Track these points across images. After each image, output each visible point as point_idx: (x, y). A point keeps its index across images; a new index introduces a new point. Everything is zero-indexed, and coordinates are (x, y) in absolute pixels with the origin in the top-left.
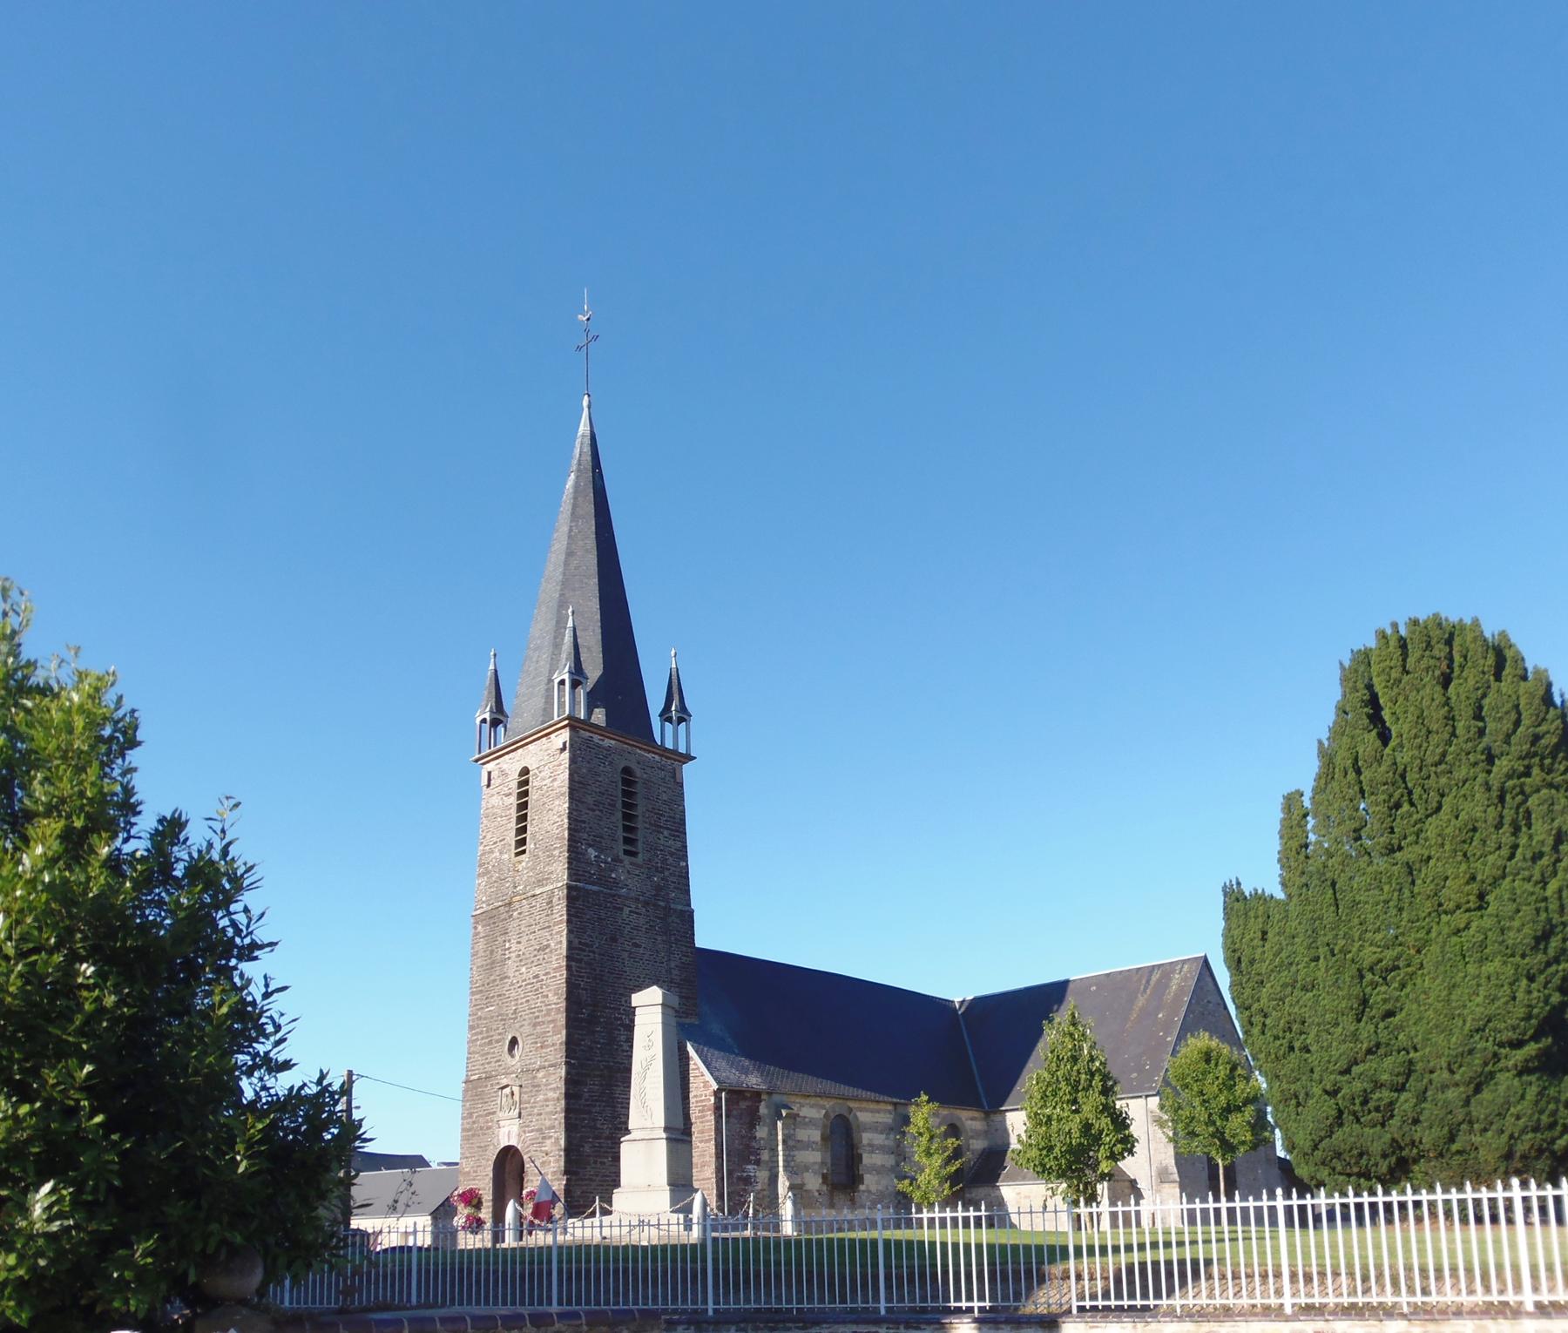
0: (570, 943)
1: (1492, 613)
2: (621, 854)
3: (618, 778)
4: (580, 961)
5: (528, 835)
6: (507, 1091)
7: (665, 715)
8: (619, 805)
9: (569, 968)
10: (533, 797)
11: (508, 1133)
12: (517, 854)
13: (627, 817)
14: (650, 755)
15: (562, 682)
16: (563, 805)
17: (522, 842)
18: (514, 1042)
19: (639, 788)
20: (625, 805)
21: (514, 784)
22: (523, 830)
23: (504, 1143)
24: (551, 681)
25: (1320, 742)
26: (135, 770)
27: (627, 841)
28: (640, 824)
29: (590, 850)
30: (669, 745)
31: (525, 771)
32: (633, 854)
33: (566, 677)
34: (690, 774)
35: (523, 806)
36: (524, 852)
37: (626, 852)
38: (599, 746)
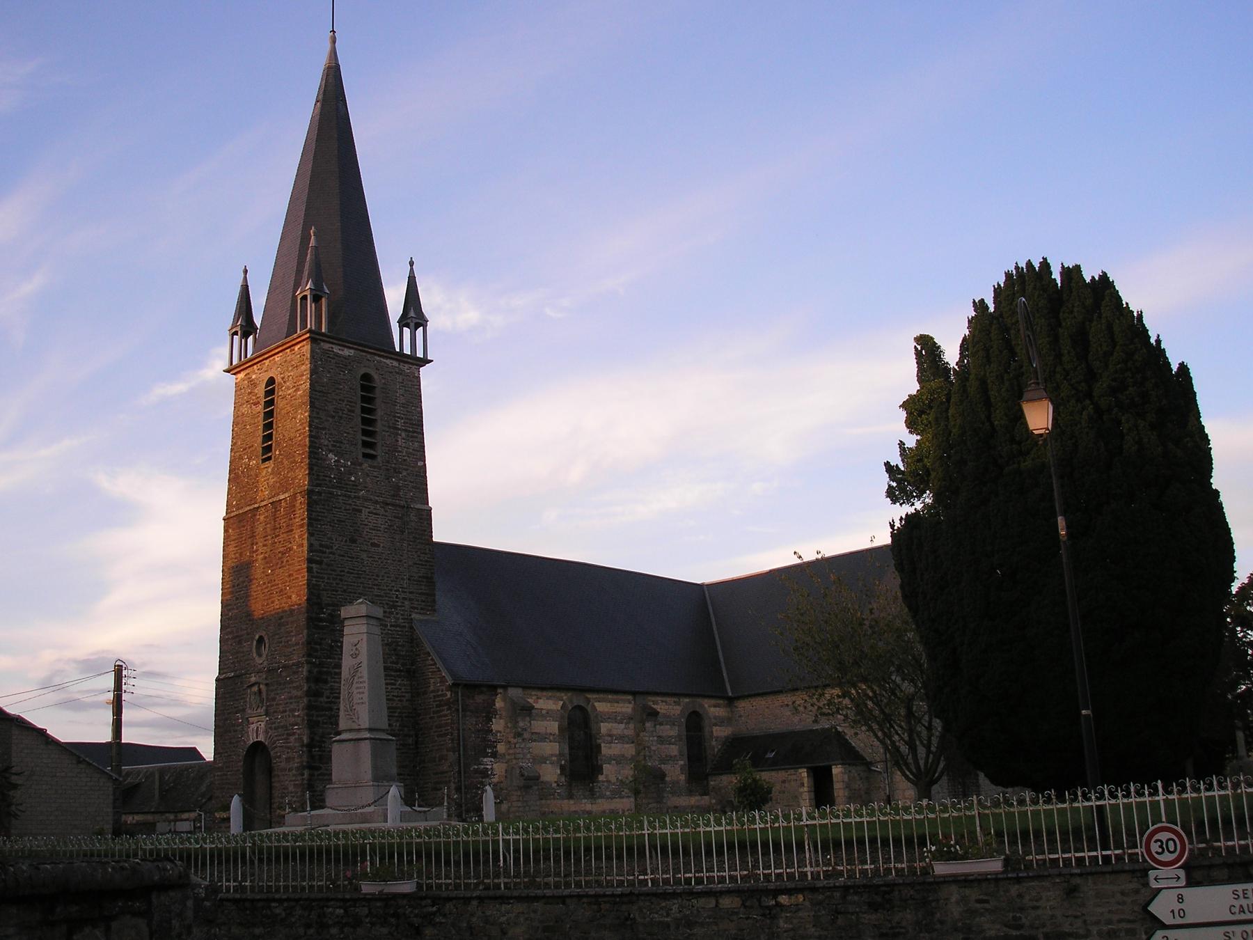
0: (310, 545)
1: (1160, 298)
2: (360, 456)
3: (357, 384)
4: (320, 563)
5: (273, 443)
6: (255, 689)
7: (403, 322)
8: (358, 411)
9: (309, 570)
10: (280, 404)
11: (256, 729)
12: (264, 461)
13: (365, 421)
14: (388, 361)
15: (305, 298)
16: (303, 415)
17: (268, 449)
18: (261, 640)
19: (378, 394)
20: (364, 410)
21: (262, 394)
22: (268, 437)
23: (252, 739)
24: (294, 297)
25: (927, 350)
26: (227, 371)
27: (366, 444)
28: (379, 427)
29: (331, 455)
30: (407, 351)
31: (271, 381)
32: (373, 457)
33: (308, 293)
34: (426, 375)
35: (269, 414)
36: (269, 458)
37: (365, 456)
38: (340, 356)
